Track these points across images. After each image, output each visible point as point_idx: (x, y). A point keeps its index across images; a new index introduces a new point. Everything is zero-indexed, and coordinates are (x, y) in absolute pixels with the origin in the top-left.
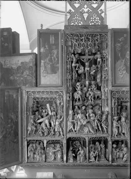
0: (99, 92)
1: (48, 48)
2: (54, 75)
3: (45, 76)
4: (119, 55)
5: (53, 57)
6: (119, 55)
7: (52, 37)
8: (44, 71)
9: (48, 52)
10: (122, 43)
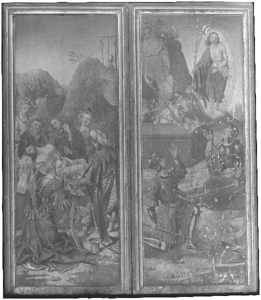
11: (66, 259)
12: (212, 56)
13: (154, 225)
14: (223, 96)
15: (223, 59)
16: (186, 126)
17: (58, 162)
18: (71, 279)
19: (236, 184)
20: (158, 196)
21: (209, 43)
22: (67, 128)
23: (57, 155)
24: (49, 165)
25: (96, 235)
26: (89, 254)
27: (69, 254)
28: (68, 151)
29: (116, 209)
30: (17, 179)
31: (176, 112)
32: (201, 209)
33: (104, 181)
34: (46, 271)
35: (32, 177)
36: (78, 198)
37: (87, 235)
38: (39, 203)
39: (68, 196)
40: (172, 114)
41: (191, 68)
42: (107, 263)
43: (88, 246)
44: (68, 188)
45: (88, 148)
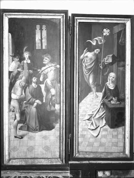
1: (29, 62)
2: (44, 133)
3: (22, 137)
5: (43, 86)
7: (41, 29)
8: (19, 122)
9: (31, 71)
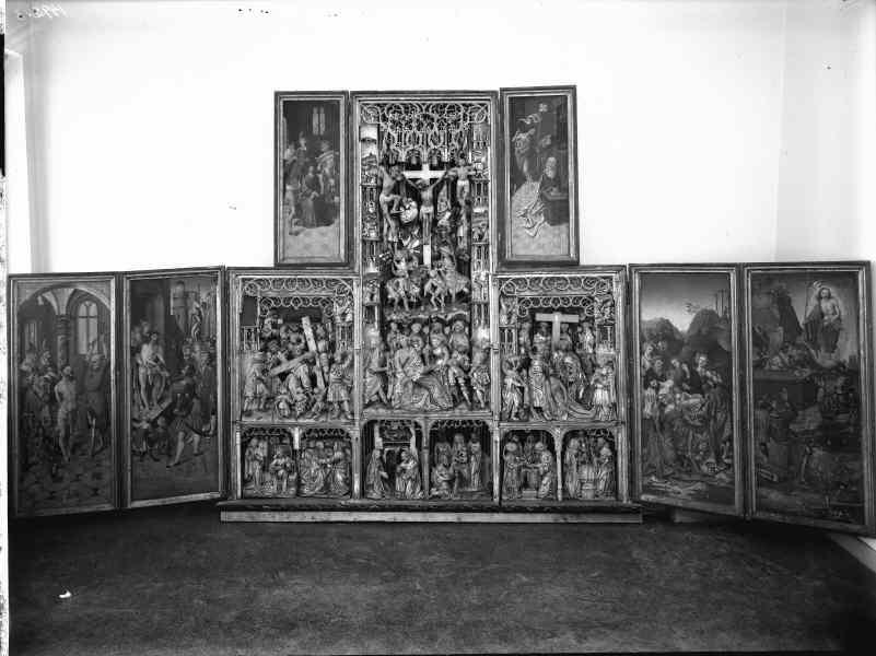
0: (463, 281)
4: (525, 169)
6: (525, 169)
10: (532, 131)
11: (686, 477)
12: (824, 310)
13: (765, 459)
14: (835, 347)
15: (835, 313)
16: (796, 373)
17: (678, 396)
18: (690, 495)
19: (851, 429)
20: (770, 432)
21: (819, 298)
22: (685, 368)
23: (676, 389)
24: (670, 396)
25: (712, 460)
26: (705, 475)
27: (689, 473)
28: (686, 387)
29: (730, 439)
30: (643, 406)
31: (786, 360)
32: (814, 449)
33: (719, 415)
34: (668, 485)
35: (656, 406)
36: (697, 427)
37: (704, 459)
38: (662, 428)
39: (685, 421)
40: (783, 362)
41: (801, 321)
42: (722, 485)
43: (705, 468)
44: (687, 417)
45: (704, 386)
